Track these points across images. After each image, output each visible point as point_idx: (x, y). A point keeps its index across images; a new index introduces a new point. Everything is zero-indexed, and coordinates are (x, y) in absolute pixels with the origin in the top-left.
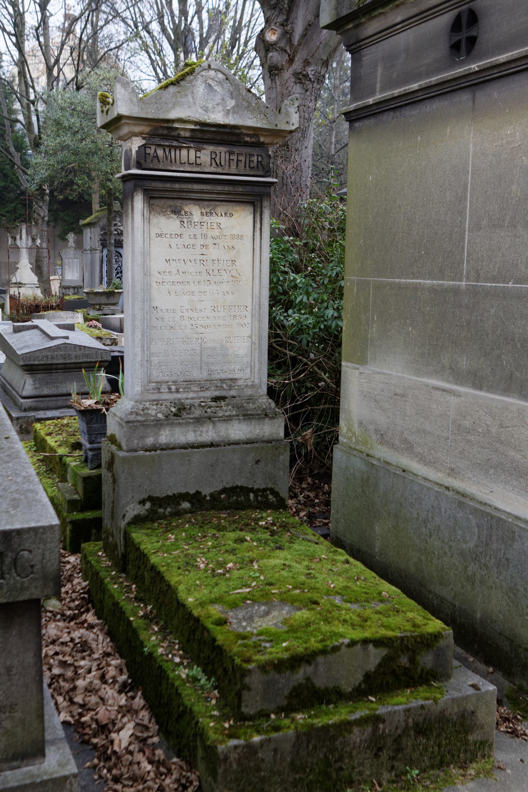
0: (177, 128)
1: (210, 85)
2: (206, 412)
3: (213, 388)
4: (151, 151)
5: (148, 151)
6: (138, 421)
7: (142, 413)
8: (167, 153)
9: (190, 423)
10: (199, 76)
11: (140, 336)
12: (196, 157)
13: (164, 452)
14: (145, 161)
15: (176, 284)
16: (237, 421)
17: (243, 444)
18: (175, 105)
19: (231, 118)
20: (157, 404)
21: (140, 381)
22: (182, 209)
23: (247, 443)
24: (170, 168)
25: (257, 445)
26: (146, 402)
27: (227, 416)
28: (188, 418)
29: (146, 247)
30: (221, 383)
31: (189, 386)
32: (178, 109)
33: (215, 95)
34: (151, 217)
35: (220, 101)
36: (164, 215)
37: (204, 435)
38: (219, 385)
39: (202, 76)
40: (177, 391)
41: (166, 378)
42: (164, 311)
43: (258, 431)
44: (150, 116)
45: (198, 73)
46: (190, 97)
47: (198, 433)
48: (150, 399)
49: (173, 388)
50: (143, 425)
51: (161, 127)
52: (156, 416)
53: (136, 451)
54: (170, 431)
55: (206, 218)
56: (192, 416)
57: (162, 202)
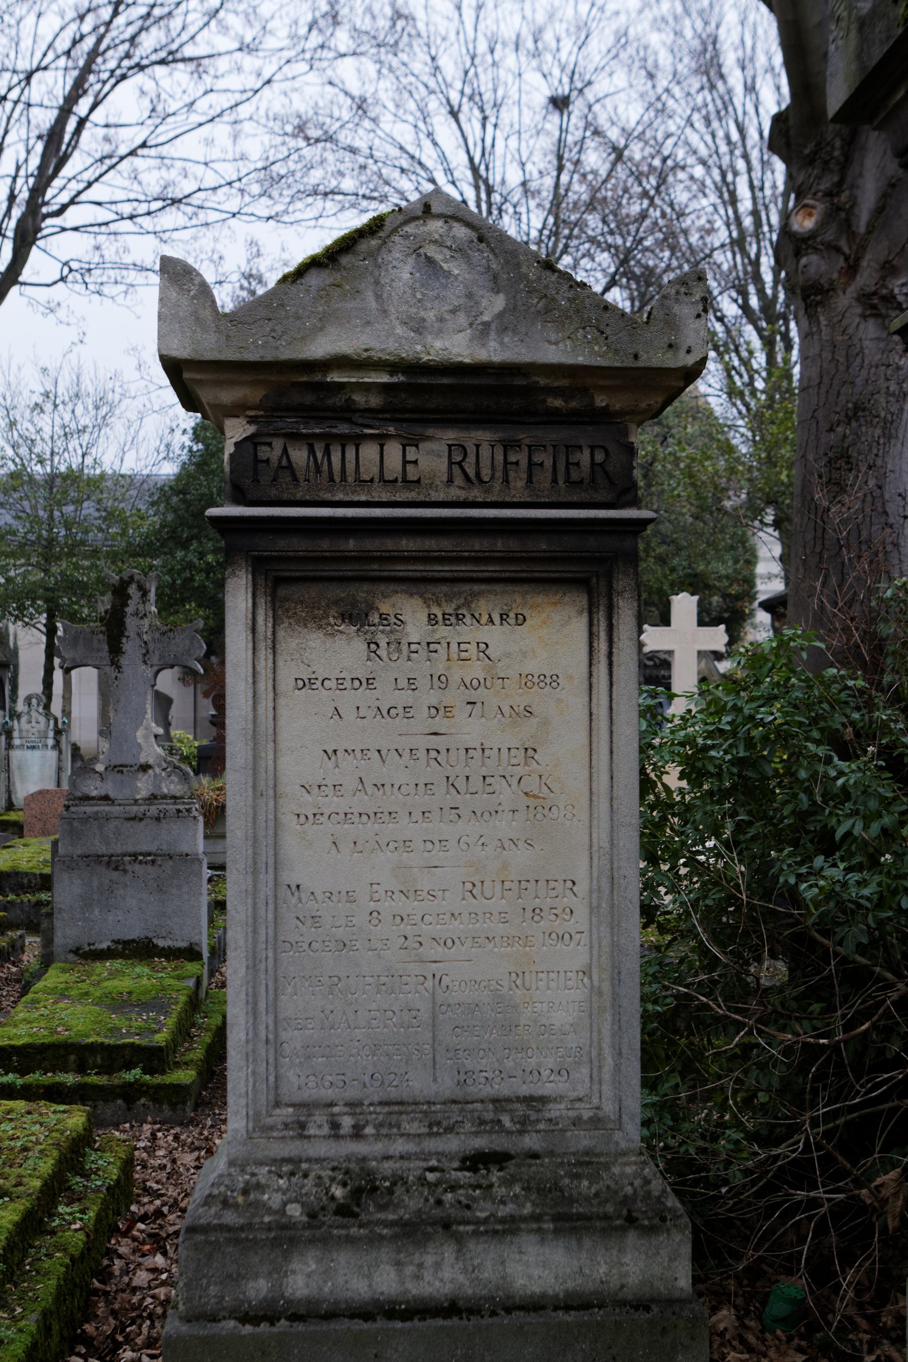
0: (341, 386)
1: (430, 260)
2: (439, 1202)
3: (468, 1126)
4: (273, 452)
5: (263, 452)
6: (222, 1228)
7: (240, 1199)
8: (319, 455)
9: (382, 1237)
10: (396, 239)
11: (242, 971)
12: (405, 462)
13: (300, 1327)
14: (256, 480)
15: (356, 818)
16: (533, 1238)
17: (556, 1308)
18: (323, 322)
19: (493, 344)
20: (292, 1174)
21: (243, 1102)
22: (372, 607)
23: (567, 1308)
24: (328, 496)
25: (599, 1315)
26: (261, 1164)
27: (502, 1221)
28: (379, 1222)
29: (262, 718)
30: (496, 1110)
31: (394, 1119)
32: (333, 331)
33: (445, 287)
34: (281, 634)
35: (462, 301)
36: (320, 627)
37: (428, 1276)
38: (488, 1116)
39: (406, 237)
40: (357, 1134)
41: (329, 1094)
42: (320, 897)
43: (603, 1269)
44: (251, 356)
45: (395, 230)
46: (369, 295)
47: (410, 1270)
48: (272, 1154)
49: (347, 1122)
50: (238, 1241)
51: (295, 385)
52: (282, 1211)
53: (214, 1318)
54: (319, 1261)
55: (442, 631)
56: (391, 1217)
57: (312, 591)
